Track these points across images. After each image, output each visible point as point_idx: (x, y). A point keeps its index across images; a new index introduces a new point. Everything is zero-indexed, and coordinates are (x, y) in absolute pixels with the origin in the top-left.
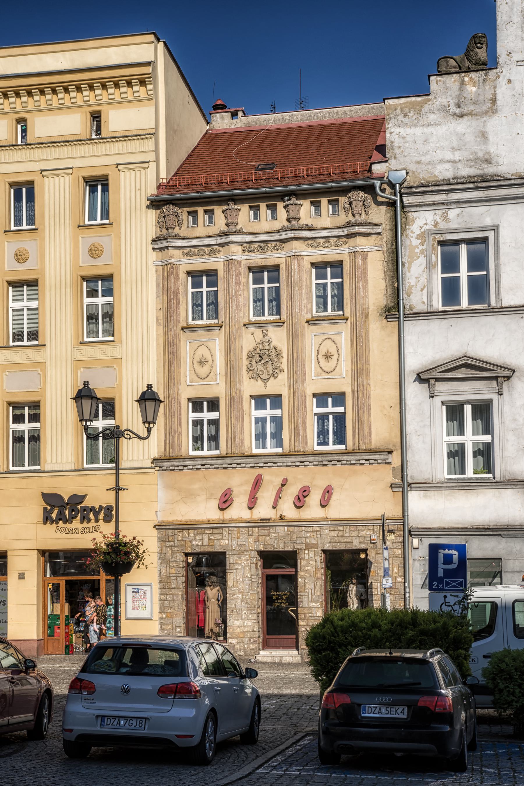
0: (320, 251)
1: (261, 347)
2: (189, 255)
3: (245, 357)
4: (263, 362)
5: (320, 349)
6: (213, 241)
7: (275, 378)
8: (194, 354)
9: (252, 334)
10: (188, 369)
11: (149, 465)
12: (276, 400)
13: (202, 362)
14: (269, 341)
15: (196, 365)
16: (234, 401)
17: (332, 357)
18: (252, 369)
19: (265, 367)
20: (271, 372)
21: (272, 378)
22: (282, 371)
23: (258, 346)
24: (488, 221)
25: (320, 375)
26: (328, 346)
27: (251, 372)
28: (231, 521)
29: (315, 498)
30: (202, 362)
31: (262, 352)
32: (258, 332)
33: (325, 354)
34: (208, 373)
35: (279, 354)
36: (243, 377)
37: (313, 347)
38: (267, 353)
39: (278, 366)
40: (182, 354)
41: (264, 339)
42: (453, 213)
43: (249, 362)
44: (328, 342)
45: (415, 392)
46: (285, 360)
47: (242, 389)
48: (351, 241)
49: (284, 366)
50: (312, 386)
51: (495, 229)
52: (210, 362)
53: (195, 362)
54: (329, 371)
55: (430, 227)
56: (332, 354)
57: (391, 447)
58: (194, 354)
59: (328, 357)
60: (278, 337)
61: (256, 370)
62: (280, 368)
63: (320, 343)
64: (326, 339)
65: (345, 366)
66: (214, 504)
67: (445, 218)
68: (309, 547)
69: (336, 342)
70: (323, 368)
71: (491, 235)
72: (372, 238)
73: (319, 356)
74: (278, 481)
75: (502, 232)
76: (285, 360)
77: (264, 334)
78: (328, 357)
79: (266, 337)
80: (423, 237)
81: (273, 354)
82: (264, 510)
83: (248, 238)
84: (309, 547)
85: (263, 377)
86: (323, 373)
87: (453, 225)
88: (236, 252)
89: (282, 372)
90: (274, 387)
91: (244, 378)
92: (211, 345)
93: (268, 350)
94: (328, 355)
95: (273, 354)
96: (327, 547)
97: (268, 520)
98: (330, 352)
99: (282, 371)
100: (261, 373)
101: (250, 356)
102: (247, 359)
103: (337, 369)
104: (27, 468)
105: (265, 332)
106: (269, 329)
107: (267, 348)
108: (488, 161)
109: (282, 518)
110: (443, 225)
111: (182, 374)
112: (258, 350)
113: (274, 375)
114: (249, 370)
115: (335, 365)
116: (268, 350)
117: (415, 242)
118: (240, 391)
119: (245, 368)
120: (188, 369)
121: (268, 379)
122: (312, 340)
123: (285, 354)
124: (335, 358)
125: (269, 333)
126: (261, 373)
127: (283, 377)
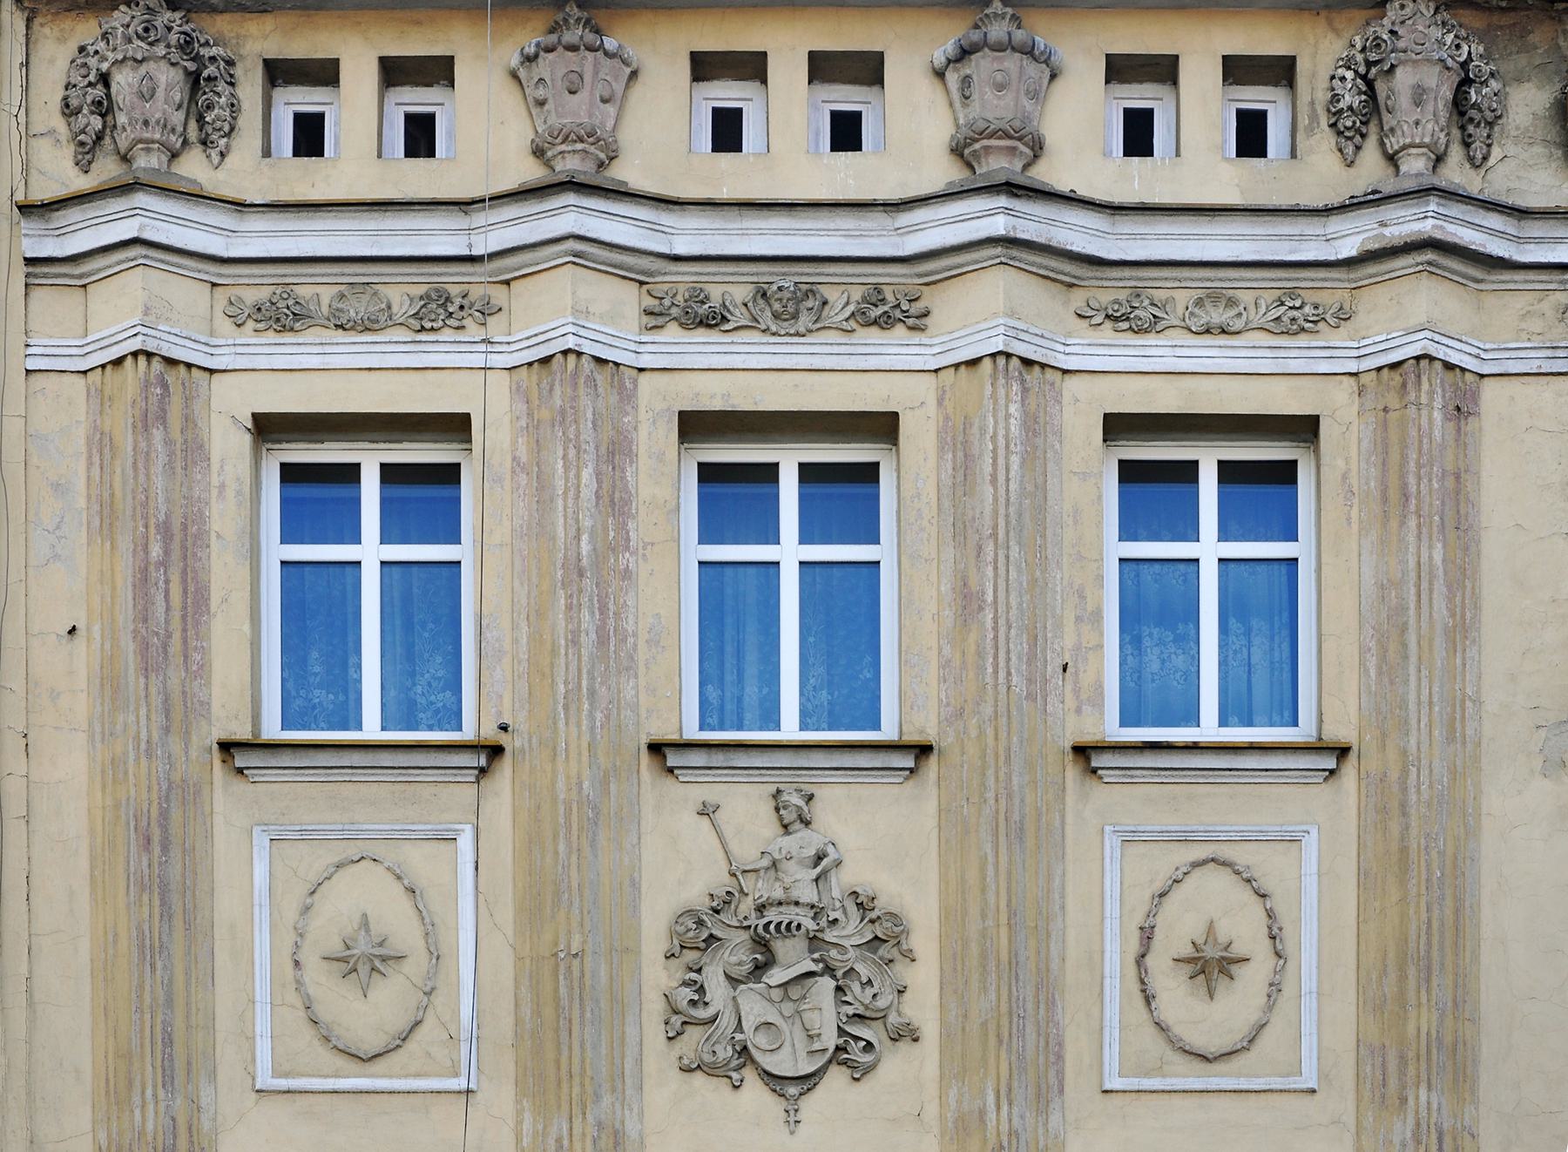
3: (654, 935)
4: (776, 976)
5: (1160, 921)
7: (860, 1073)
8: (307, 909)
9: (706, 811)
10: (262, 991)
13: (364, 961)
14: (819, 858)
17: (1234, 969)
18: (702, 1013)
19: (788, 1008)
20: (830, 1040)
22: (906, 1034)
23: (747, 883)
25: (1159, 1071)
26: (1213, 907)
27: (693, 1033)
30: (364, 961)
31: (772, 915)
32: (746, 809)
33: (1188, 951)
34: (403, 1023)
35: (887, 939)
36: (639, 1061)
37: (1112, 908)
38: (809, 924)
39: (881, 1003)
40: (226, 906)
41: (789, 843)
43: (681, 975)
44: (1216, 883)
47: (632, 1128)
52: (417, 965)
53: (310, 959)
54: (1213, 1046)
56: (1238, 950)
58: (307, 909)
60: (881, 840)
62: (893, 1019)
63: (1158, 886)
64: (1196, 865)
69: (1267, 885)
70: (1177, 1030)
73: (1150, 961)
77: (789, 816)
79: (802, 834)
81: (851, 932)
85: (781, 1064)
86: (1178, 1058)
89: (904, 1046)
91: (650, 1065)
92: (419, 860)
93: (817, 911)
94: (1211, 952)
95: (851, 932)
98: (1222, 939)
99: (906, 1034)
100: (762, 1040)
102: (670, 956)
103: (1267, 1040)
105: (796, 800)
106: (819, 792)
107: (808, 894)
111: (224, 1023)
112: (746, 906)
114: (685, 1017)
115: (1255, 1017)
116: (817, 911)
119: (654, 1008)
120: (262, 991)
121: (808, 1081)
122: (1109, 863)
123: (924, 939)
124: (1253, 979)
125: (822, 813)
126: (762, 1040)
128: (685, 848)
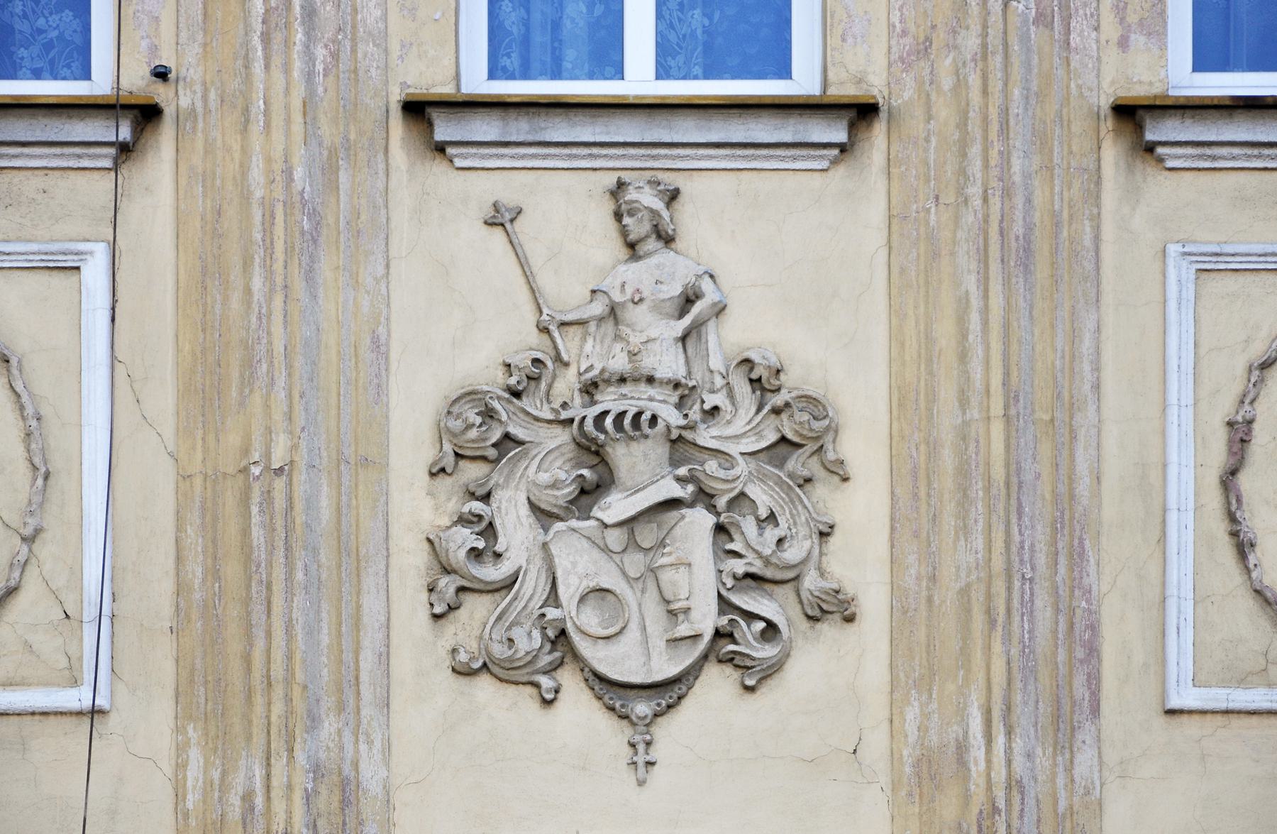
1: (592, 354)
3: (411, 440)
4: (616, 507)
7: (755, 677)
9: (501, 219)
14: (689, 299)
18: (491, 573)
19: (635, 563)
20: (706, 619)
21: (717, 684)
22: (833, 609)
23: (568, 344)
27: (477, 609)
31: (609, 400)
32: (566, 210)
35: (801, 442)
36: (385, 657)
37: (1180, 389)
38: (671, 416)
39: (792, 554)
41: (638, 275)
47: (371, 775)
49: (861, 559)
60: (795, 269)
61: (532, 587)
62: (811, 582)
73: (1245, 481)
77: (638, 227)
81: (739, 430)
85: (621, 661)
89: (829, 630)
91: (403, 664)
93: (684, 393)
95: (739, 430)
99: (833, 609)
100: (590, 619)
102: (438, 472)
105: (650, 199)
107: (668, 363)
112: (566, 385)
114: (458, 582)
116: (684, 393)
118: (348, 791)
119: (411, 561)
121: (669, 691)
123: (864, 443)
125: (692, 221)
126: (590, 619)
128: (465, 280)
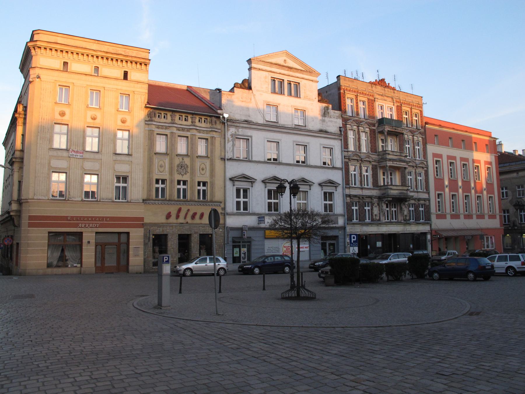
0: (201, 134)
2: (158, 128)
6: (167, 125)
11: (142, 202)
12: (185, 183)
13: (161, 166)
15: (159, 167)
16: (172, 181)
24: (249, 134)
26: (203, 166)
28: (170, 223)
29: (198, 216)
30: (161, 166)
32: (181, 158)
35: (187, 167)
42: (240, 130)
45: (229, 184)
46: (189, 169)
48: (211, 133)
50: (197, 179)
51: (251, 137)
55: (233, 133)
57: (221, 200)
59: (203, 169)
65: (208, 174)
66: (164, 217)
67: (238, 131)
68: (196, 233)
71: (250, 138)
72: (217, 133)
74: (186, 209)
75: (253, 138)
76: (189, 169)
78: (203, 169)
80: (232, 135)
82: (181, 220)
83: (179, 126)
84: (196, 233)
87: (240, 133)
88: (174, 130)
90: (185, 178)
92: (164, 160)
96: (201, 233)
97: (183, 223)
101: (178, 166)
104: (90, 199)
108: (249, 116)
109: (187, 223)
110: (237, 133)
113: (186, 174)
114: (177, 171)
117: (230, 137)
127: (188, 174)
